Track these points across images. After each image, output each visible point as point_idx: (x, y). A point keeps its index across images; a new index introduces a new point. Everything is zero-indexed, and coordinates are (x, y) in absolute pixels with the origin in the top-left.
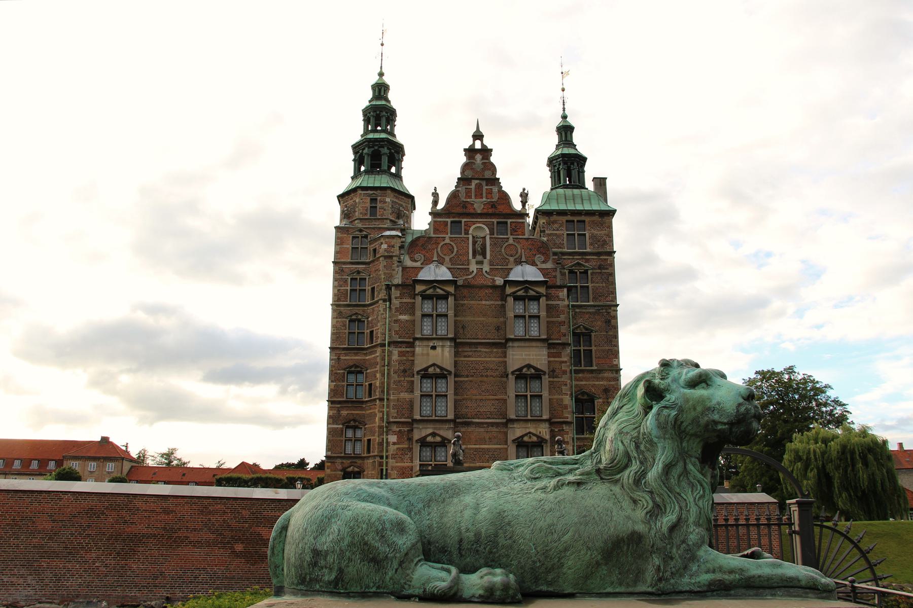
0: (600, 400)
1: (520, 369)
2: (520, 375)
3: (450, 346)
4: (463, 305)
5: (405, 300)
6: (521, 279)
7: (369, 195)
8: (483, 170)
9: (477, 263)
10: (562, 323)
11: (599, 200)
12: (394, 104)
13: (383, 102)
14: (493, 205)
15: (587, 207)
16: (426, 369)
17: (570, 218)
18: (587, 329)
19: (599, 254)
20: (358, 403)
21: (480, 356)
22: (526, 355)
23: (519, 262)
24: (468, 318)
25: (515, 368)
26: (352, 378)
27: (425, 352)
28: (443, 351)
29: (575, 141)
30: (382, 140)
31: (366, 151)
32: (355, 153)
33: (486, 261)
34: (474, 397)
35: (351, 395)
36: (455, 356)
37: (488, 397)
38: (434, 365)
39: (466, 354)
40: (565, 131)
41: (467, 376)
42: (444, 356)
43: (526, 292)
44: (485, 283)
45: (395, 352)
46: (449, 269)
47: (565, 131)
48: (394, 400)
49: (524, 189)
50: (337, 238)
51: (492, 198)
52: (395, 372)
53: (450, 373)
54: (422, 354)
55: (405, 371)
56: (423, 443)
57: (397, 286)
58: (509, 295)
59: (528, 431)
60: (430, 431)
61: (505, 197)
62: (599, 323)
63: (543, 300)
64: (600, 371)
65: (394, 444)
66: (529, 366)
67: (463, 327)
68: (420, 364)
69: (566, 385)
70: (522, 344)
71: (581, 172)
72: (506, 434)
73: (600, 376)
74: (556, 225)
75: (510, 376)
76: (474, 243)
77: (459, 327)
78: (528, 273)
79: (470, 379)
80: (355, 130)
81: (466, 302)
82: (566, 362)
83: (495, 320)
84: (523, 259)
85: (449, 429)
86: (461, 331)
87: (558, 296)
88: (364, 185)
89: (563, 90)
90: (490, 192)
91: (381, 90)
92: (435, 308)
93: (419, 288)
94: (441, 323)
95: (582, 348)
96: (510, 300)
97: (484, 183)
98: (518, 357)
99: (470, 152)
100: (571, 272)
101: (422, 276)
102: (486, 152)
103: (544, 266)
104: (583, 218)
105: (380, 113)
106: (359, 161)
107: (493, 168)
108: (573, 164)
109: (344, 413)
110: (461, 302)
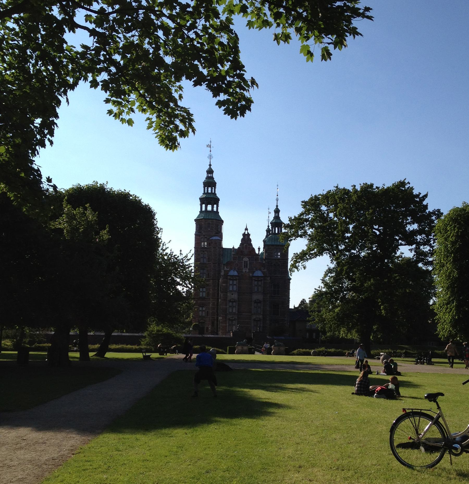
2: (255, 302)
20: (203, 298)
23: (257, 270)
26: (201, 289)
29: (280, 216)
30: (212, 198)
35: (201, 296)
38: (233, 299)
42: (235, 296)
45: (222, 294)
56: (229, 319)
61: (253, 249)
63: (262, 282)
66: (258, 300)
78: (258, 273)
80: (200, 192)
90: (249, 248)
91: (210, 171)
92: (233, 283)
93: (229, 277)
94: (235, 286)
98: (255, 297)
99: (244, 235)
102: (248, 235)
105: (210, 183)
107: (250, 240)
109: (199, 302)
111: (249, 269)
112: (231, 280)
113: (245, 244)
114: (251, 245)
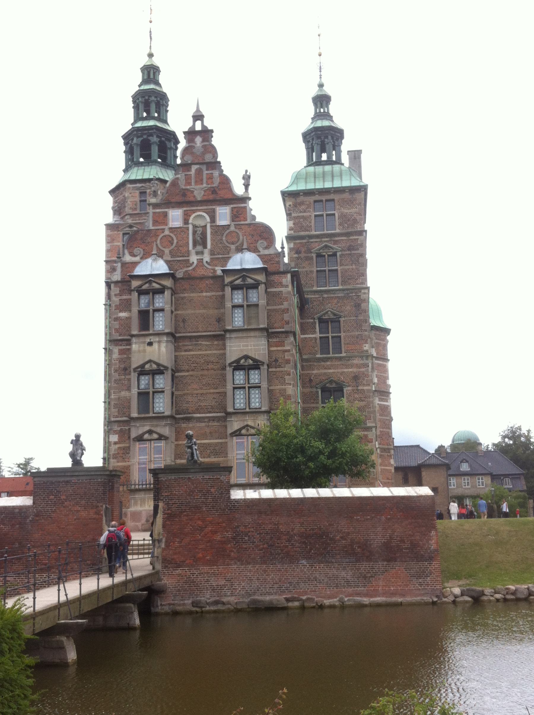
0: (349, 388)
1: (238, 361)
2: (237, 366)
3: (167, 341)
4: (183, 298)
5: (124, 297)
6: (239, 267)
7: (138, 189)
8: (203, 154)
9: (197, 253)
10: (287, 310)
11: (351, 175)
12: (165, 89)
13: (152, 86)
14: (214, 191)
15: (337, 184)
16: (143, 366)
17: (317, 197)
18: (335, 315)
19: (348, 234)
21: (200, 350)
22: (243, 346)
23: (240, 250)
24: (190, 312)
25: (233, 360)
27: (141, 348)
28: (159, 346)
31: (135, 141)
32: (126, 144)
33: (206, 251)
34: (195, 392)
36: (176, 351)
37: (209, 391)
38: (150, 361)
39: (186, 348)
40: (322, 101)
41: (188, 371)
42: (160, 351)
43: (244, 280)
44: (206, 274)
46: (167, 262)
47: (322, 101)
48: (115, 399)
49: (246, 171)
50: (108, 236)
51: (212, 183)
52: (116, 371)
53: (166, 368)
54: (139, 351)
55: (125, 369)
57: (116, 282)
58: (227, 285)
59: (246, 423)
60: (147, 428)
61: (226, 181)
62: (348, 308)
63: (262, 287)
64: (349, 358)
65: (115, 443)
66: (246, 357)
67: (184, 321)
68: (136, 361)
69: (289, 374)
70: (240, 334)
71: (336, 146)
72: (226, 427)
73: (349, 363)
74: (303, 207)
75: (228, 368)
76: (194, 232)
77: (178, 321)
79: (191, 373)
81: (186, 295)
82: (288, 351)
83: (216, 311)
84: (245, 246)
85: (165, 425)
86: (182, 325)
87: (281, 283)
88: (133, 177)
89: (320, 55)
90: (210, 177)
95: (330, 335)
96: (228, 290)
97: (204, 167)
98: (236, 348)
100: (319, 256)
101: (140, 270)
102: (207, 133)
103: (267, 252)
104: (332, 196)
106: (130, 152)
107: (213, 151)
108: (327, 137)
110: (182, 295)
111: (212, 253)
112: (146, 292)
113: (194, 168)
114: (215, 165)
